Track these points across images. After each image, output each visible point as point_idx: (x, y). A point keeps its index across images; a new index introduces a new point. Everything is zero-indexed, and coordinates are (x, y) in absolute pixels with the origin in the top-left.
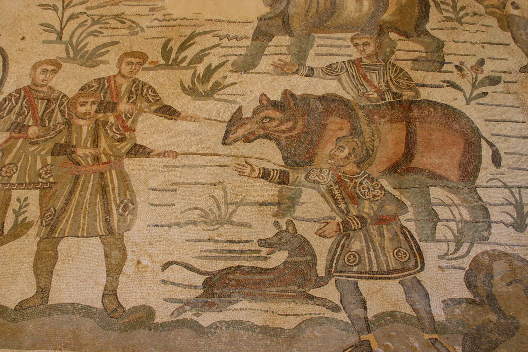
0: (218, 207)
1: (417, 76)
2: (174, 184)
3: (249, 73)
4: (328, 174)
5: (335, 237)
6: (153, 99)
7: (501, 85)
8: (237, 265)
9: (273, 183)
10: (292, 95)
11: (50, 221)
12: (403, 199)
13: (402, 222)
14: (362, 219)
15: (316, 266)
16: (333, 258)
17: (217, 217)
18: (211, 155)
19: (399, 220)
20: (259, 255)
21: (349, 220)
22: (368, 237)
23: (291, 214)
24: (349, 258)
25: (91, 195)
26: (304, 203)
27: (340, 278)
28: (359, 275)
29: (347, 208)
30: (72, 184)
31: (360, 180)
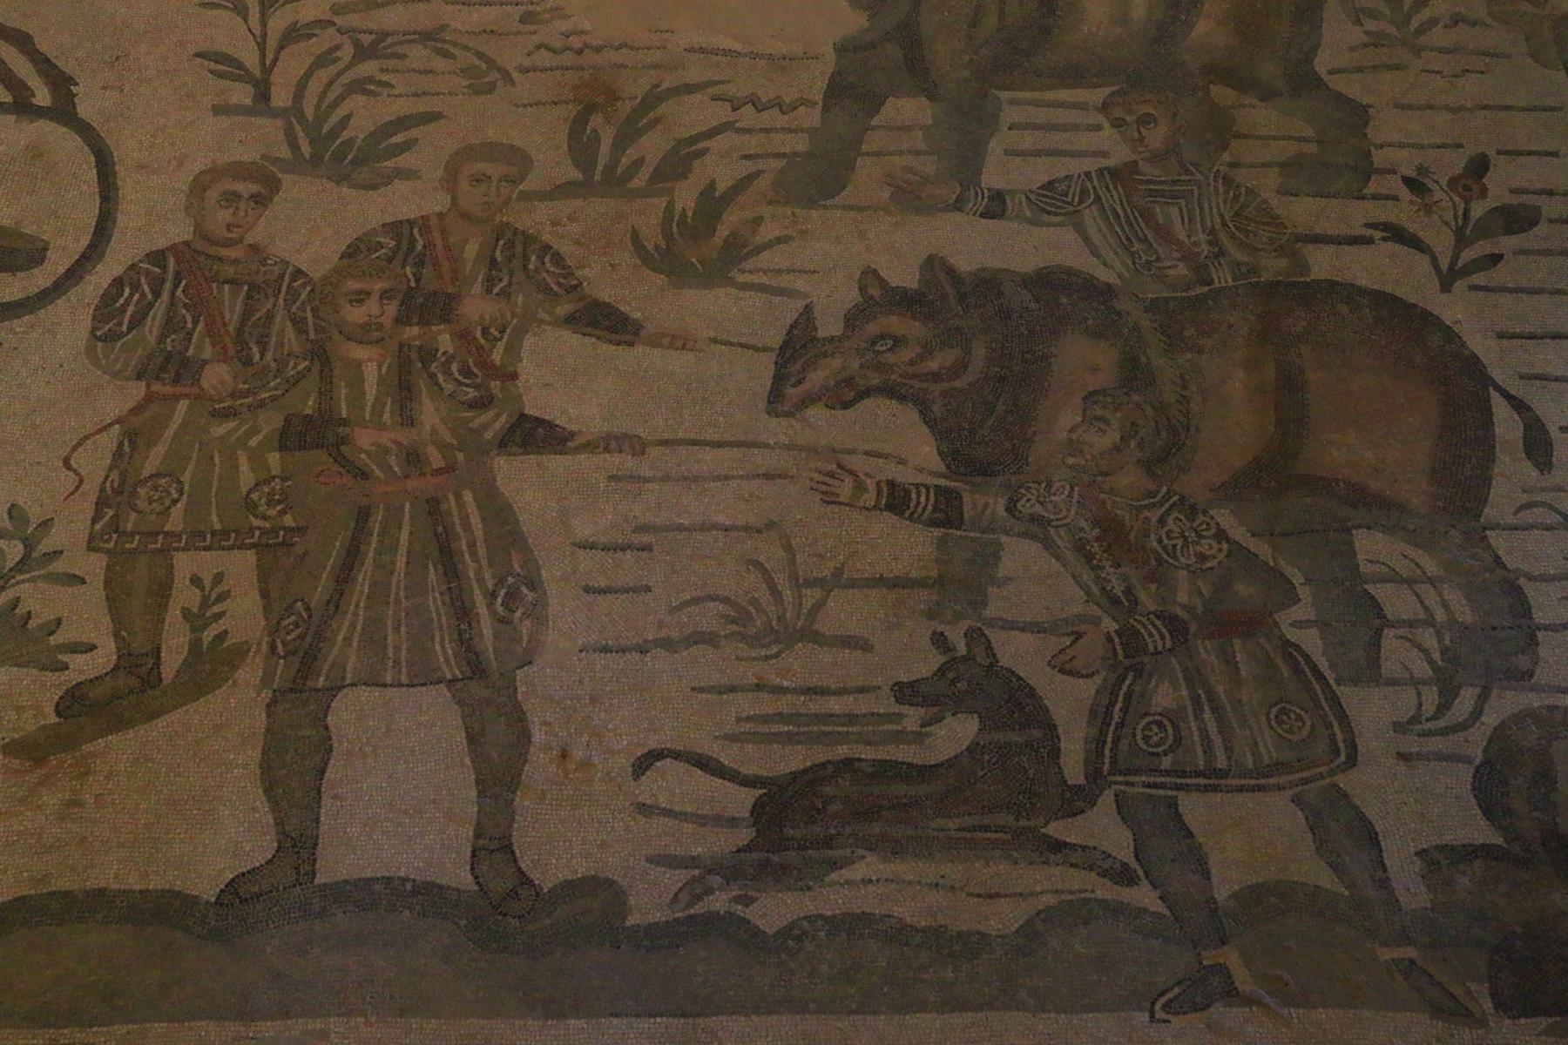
1: (1304, 211)
2: (642, 529)
3: (825, 208)
4: (1070, 496)
5: (1104, 674)
6: (559, 284)
7: (1542, 229)
8: (843, 756)
9: (919, 520)
10: (951, 271)
11: (298, 642)
14: (1172, 621)
15: (1058, 757)
17: (774, 623)
18: (739, 444)
19: (1276, 625)
20: (900, 728)
21: (1139, 627)
24: (1146, 733)
25: (408, 563)
27: (1128, 789)
29: (1129, 591)
30: (349, 533)
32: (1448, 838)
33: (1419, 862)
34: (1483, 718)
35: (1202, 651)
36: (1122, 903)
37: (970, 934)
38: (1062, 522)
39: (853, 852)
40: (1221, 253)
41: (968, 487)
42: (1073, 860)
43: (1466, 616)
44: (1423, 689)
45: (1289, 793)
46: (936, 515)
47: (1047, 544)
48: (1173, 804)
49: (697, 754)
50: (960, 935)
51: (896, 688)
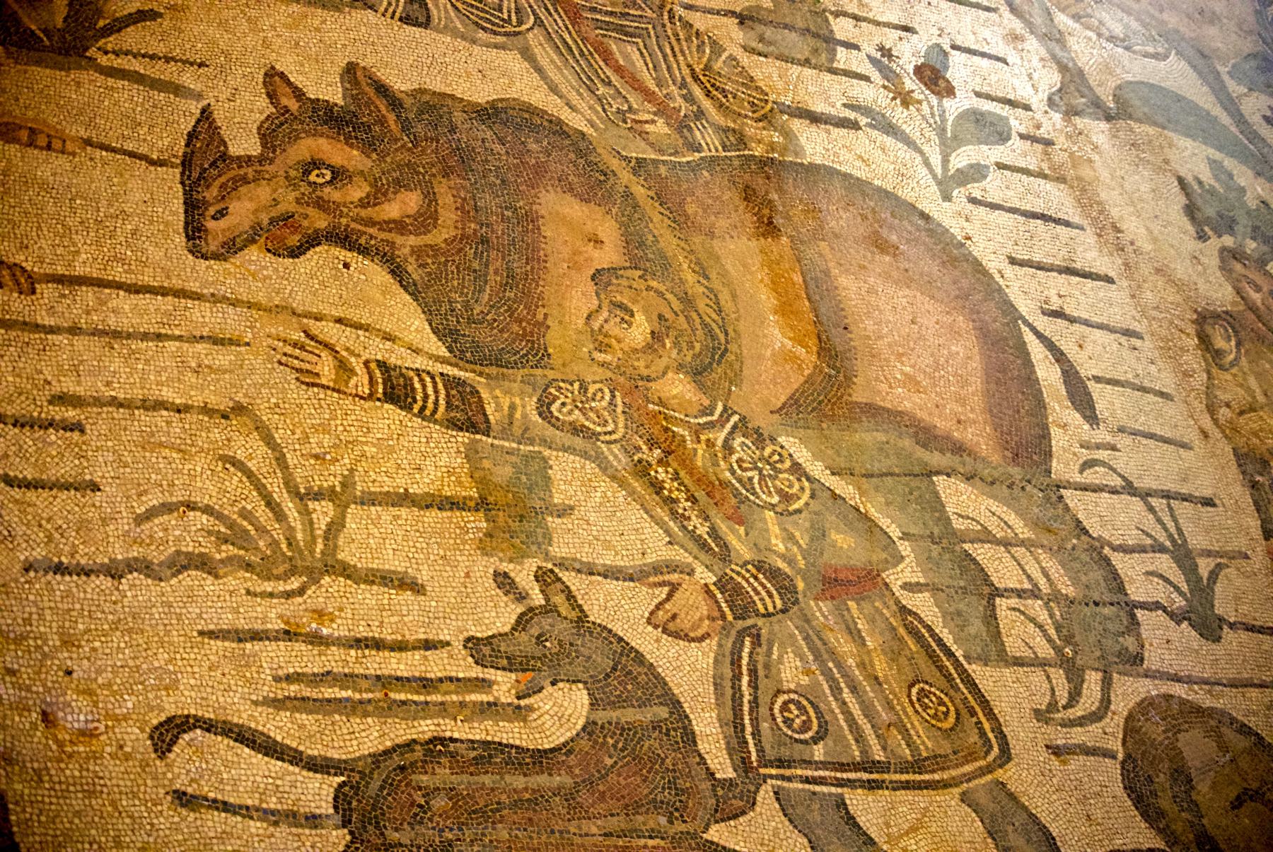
20: (491, 699)
23: (539, 545)
26: (572, 508)
28: (839, 775)
31: (721, 436)
34: (1112, 707)
40: (700, 114)
44: (1051, 670)
45: (956, 791)
48: (841, 804)
49: (237, 725)
51: (470, 645)
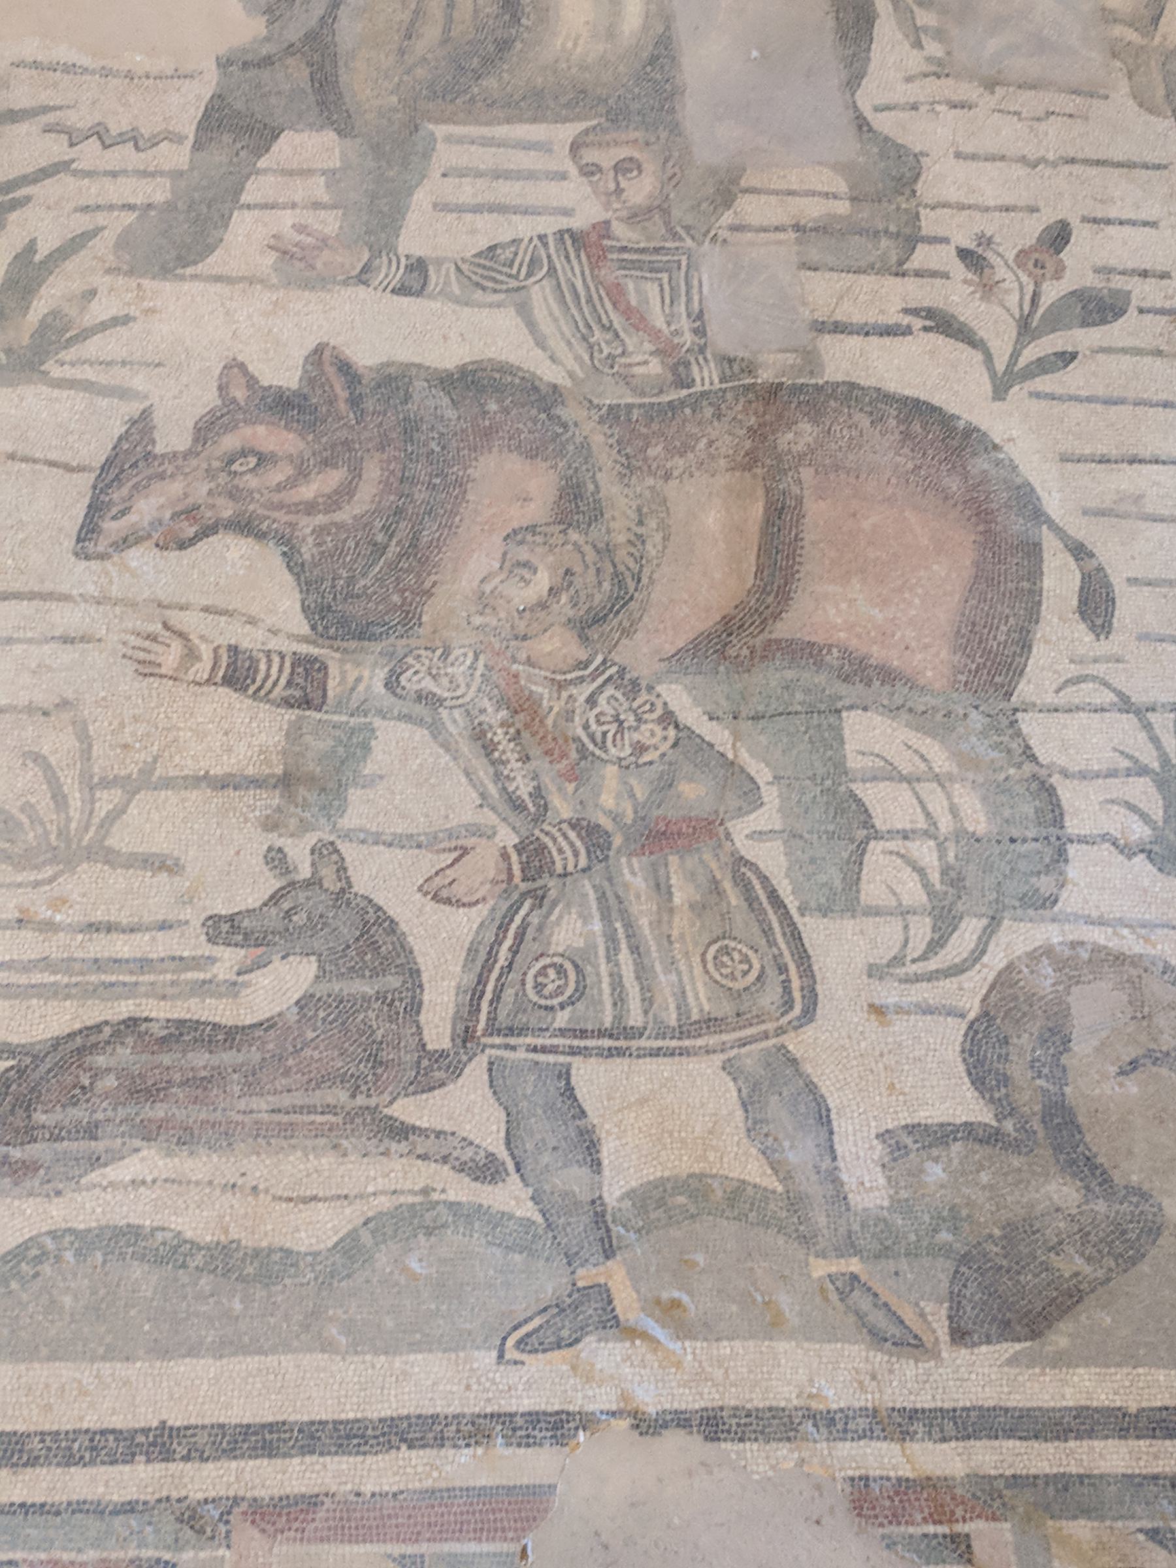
0: (60, 800)
5: (492, 902)
8: (125, 1016)
12: (745, 757)
13: (738, 844)
15: (418, 1012)
16: (482, 981)
17: (53, 837)
19: (728, 835)
20: (208, 976)
21: (546, 840)
22: (612, 901)
24: (540, 979)
26: (381, 777)
29: (538, 793)
32: (924, 1115)
33: (880, 1147)
34: (985, 959)
35: (626, 871)
36: (480, 1206)
37: (271, 1251)
38: (460, 701)
39: (124, 1144)
41: (338, 655)
42: (420, 1151)
43: (978, 820)
45: (718, 1059)
46: (289, 692)
47: (435, 729)
48: (565, 1074)
50: (257, 1253)
51: (210, 923)
